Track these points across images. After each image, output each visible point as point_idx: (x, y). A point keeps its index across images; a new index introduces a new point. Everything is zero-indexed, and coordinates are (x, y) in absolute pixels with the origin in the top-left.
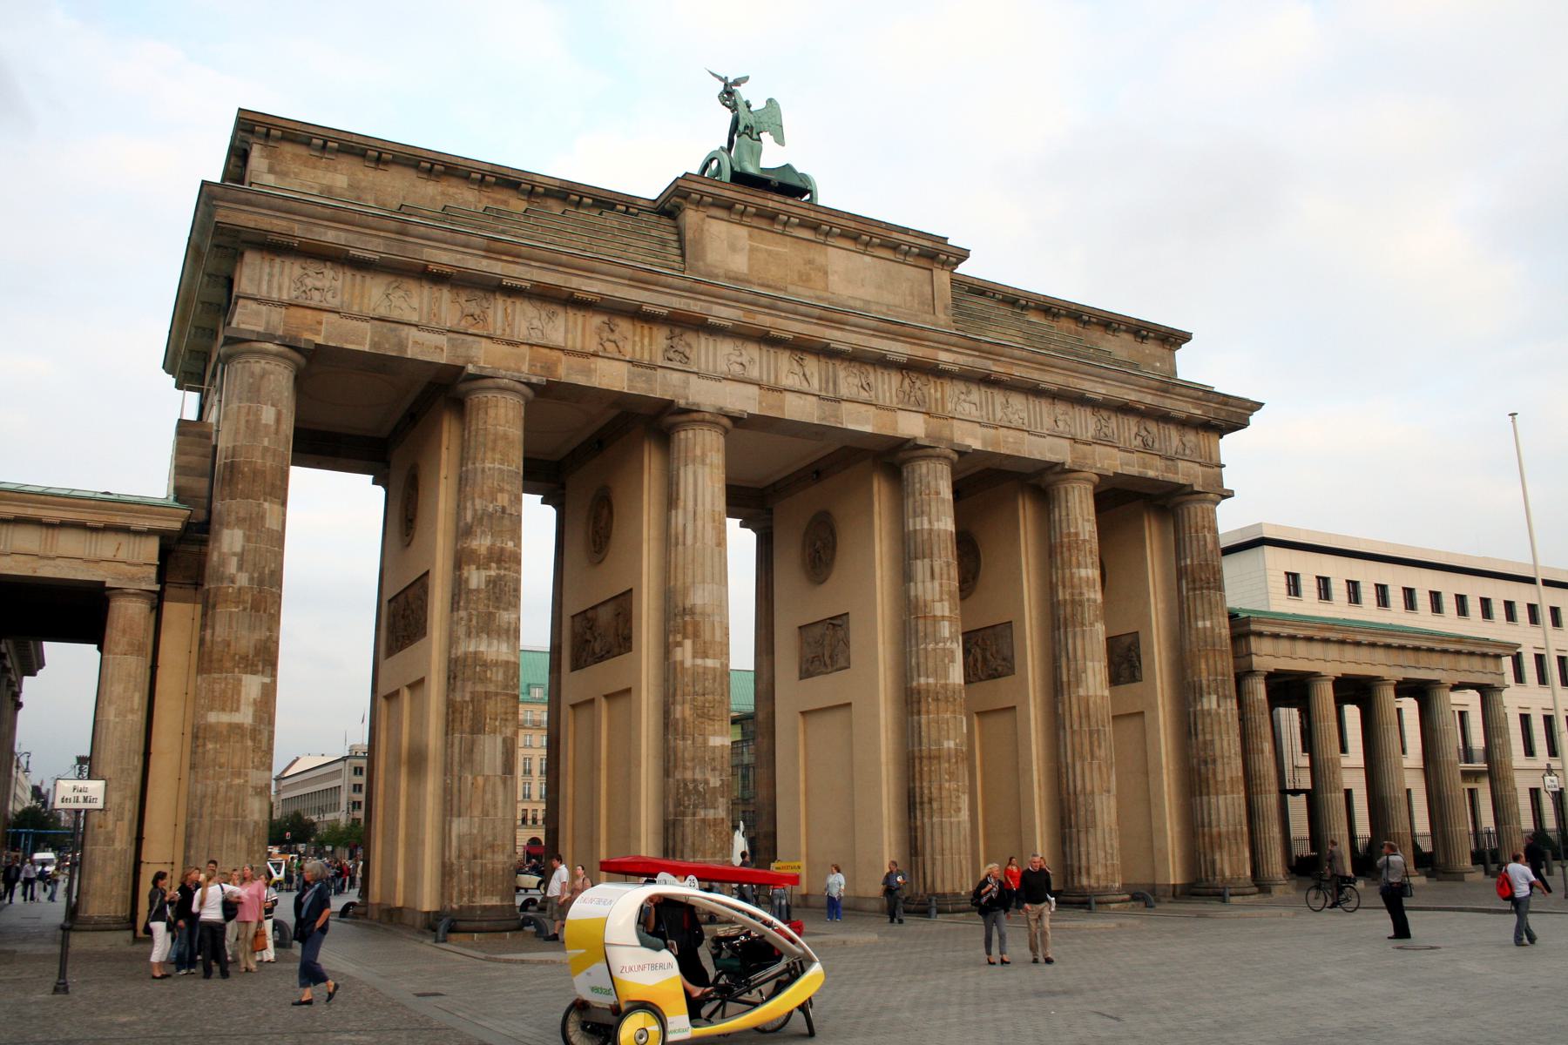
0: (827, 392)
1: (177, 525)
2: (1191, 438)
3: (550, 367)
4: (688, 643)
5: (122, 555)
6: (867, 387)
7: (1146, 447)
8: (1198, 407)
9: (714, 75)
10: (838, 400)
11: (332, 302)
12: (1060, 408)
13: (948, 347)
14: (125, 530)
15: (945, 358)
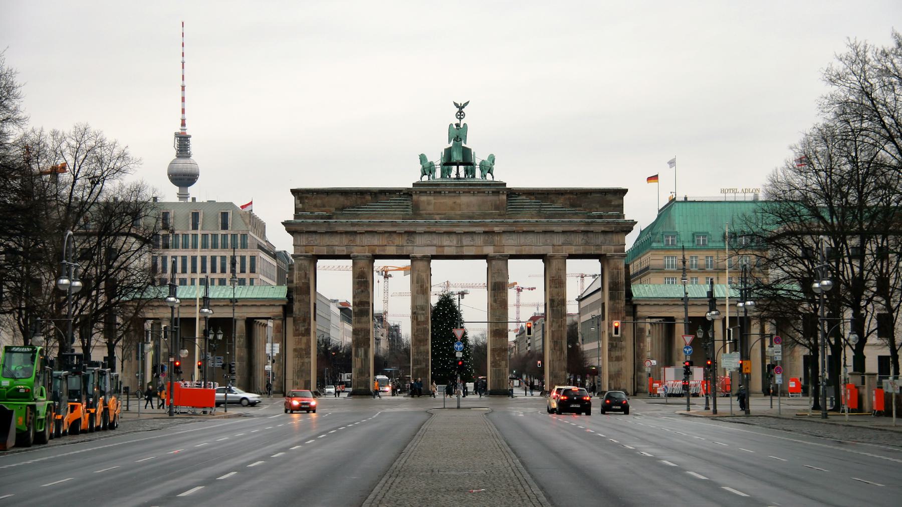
0: (458, 244)
1: (285, 303)
2: (610, 236)
3: (373, 251)
4: (415, 322)
5: (274, 311)
6: (473, 240)
7: (587, 244)
8: (607, 227)
9: (456, 104)
10: (463, 246)
11: (316, 243)
12: (548, 236)
13: (497, 226)
14: (274, 305)
15: (496, 229)
